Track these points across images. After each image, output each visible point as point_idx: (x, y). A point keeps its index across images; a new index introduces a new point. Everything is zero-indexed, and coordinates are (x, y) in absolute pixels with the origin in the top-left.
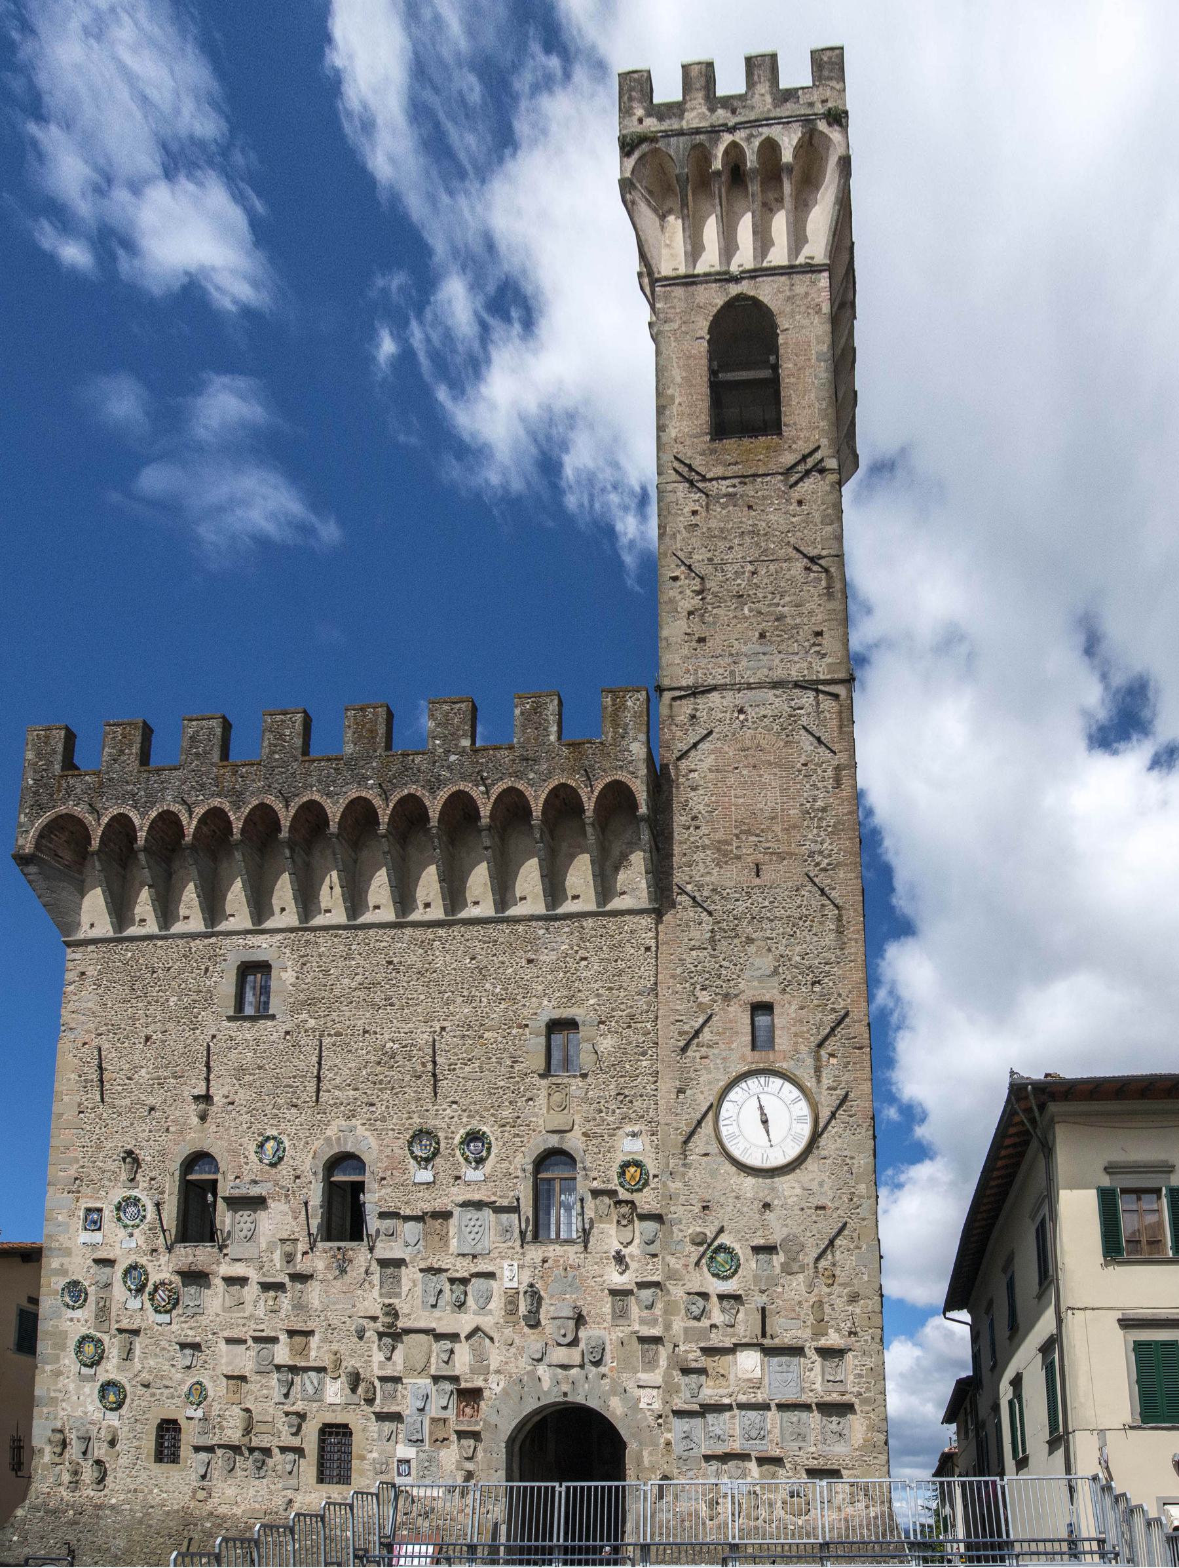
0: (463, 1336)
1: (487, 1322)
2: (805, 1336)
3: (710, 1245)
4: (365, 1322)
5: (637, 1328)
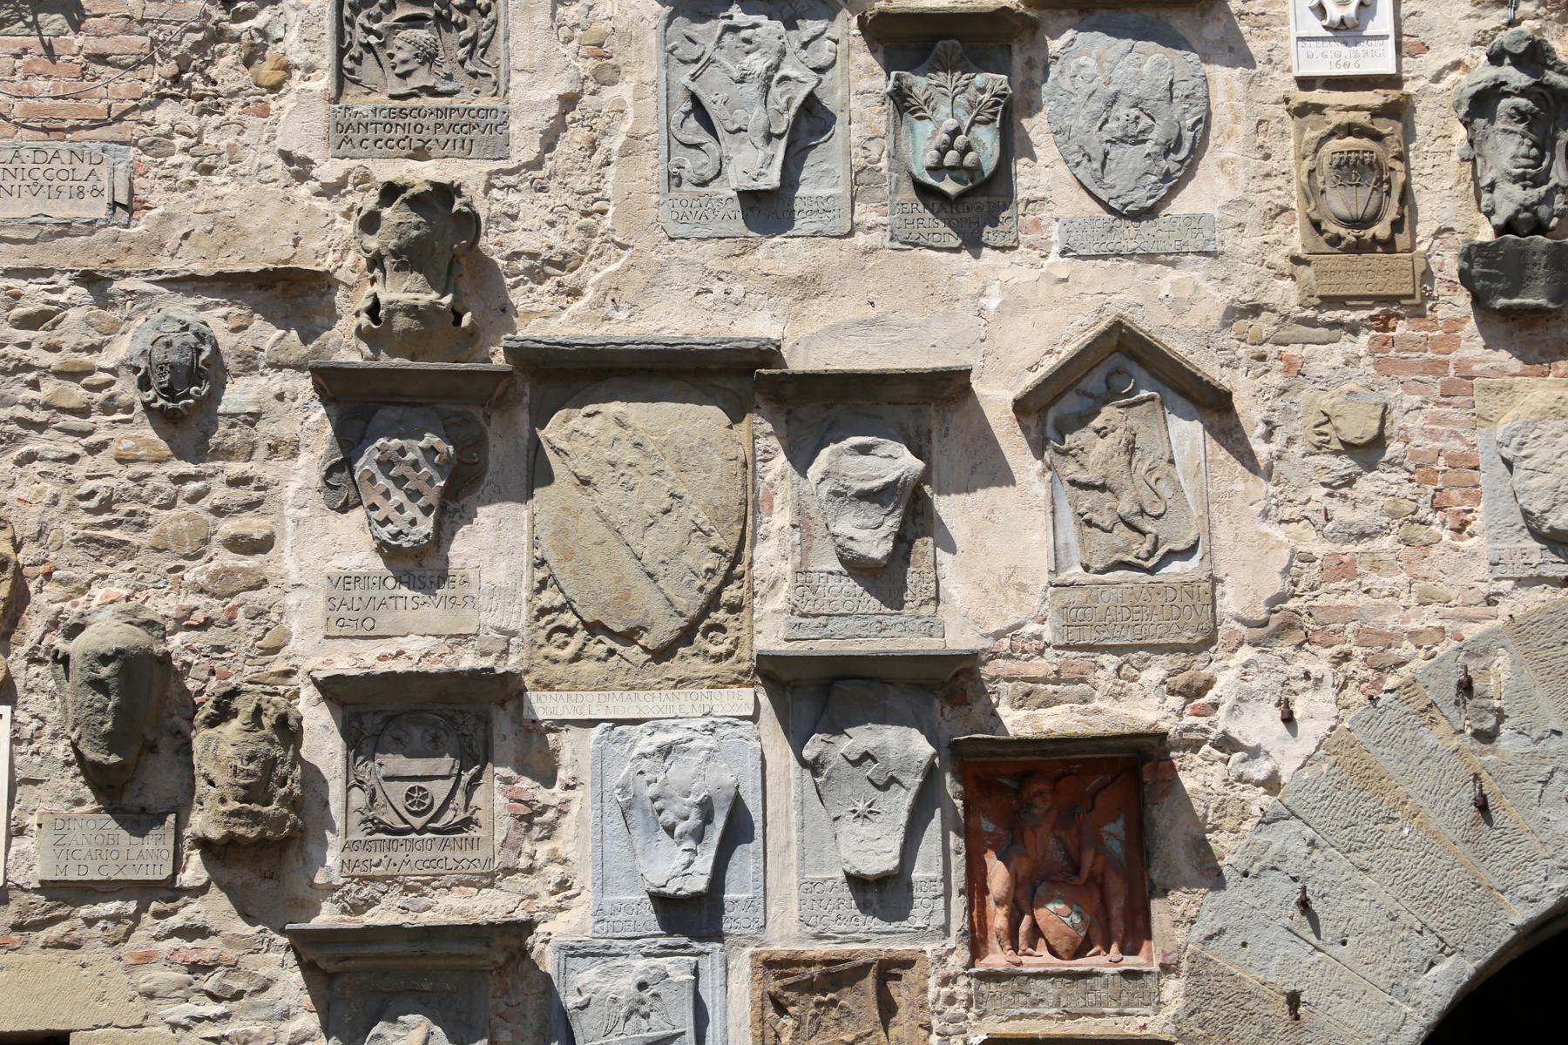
0: (996, 396)
1: (1177, 307)
4: (218, 319)
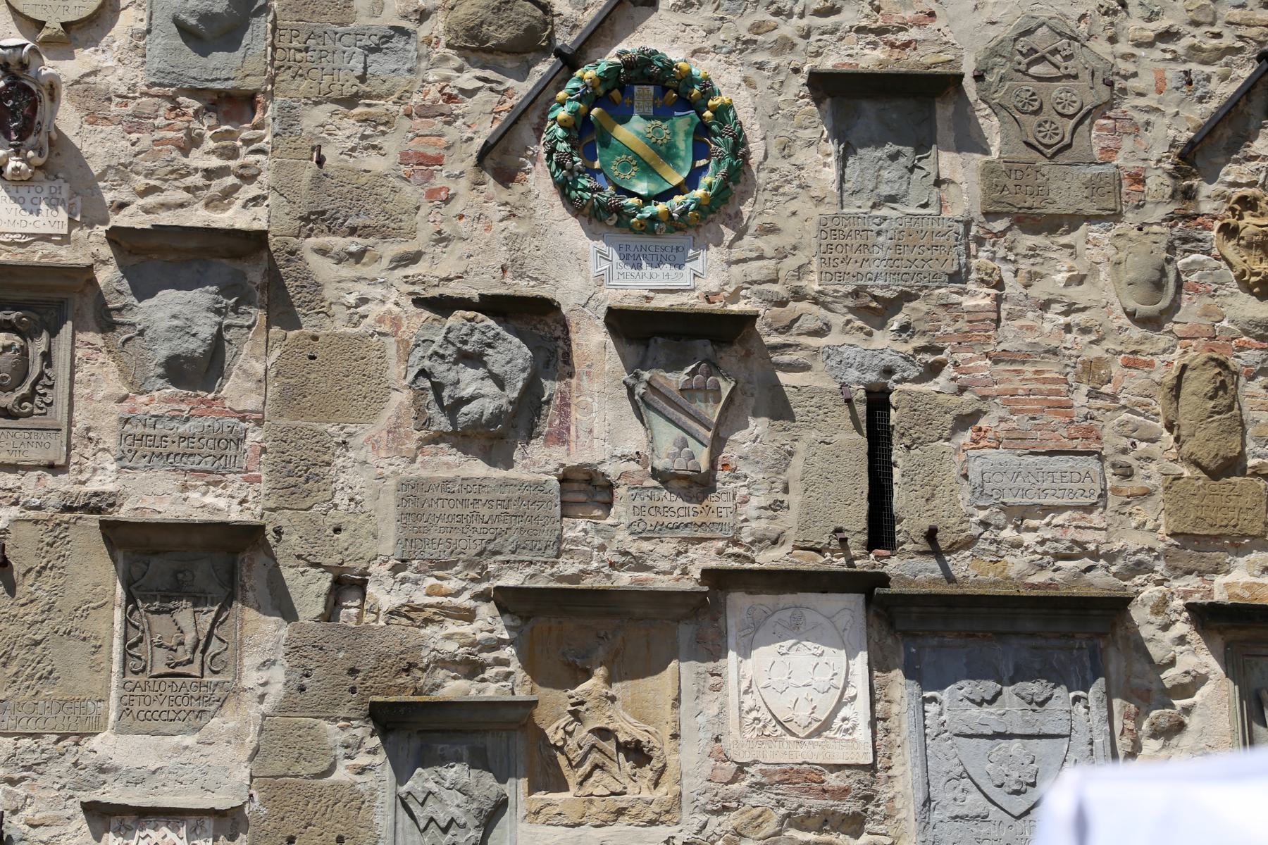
2: (1130, 541)
3: (571, 61)
5: (104, 481)
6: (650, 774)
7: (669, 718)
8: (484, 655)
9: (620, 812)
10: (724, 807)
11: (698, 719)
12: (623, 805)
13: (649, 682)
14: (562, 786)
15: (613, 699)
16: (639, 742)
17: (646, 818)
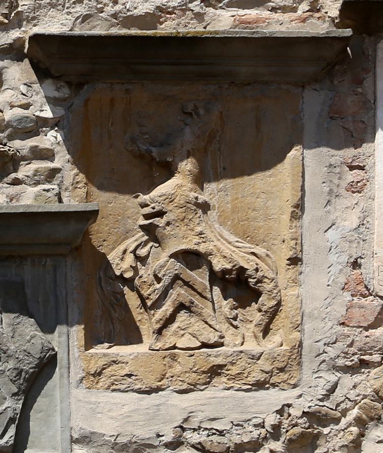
6: (258, 317)
7: (286, 233)
8: (17, 144)
9: (215, 371)
10: (362, 361)
11: (327, 238)
12: (219, 361)
13: (259, 181)
14: (132, 336)
15: (205, 207)
16: (242, 270)
17: (251, 380)
